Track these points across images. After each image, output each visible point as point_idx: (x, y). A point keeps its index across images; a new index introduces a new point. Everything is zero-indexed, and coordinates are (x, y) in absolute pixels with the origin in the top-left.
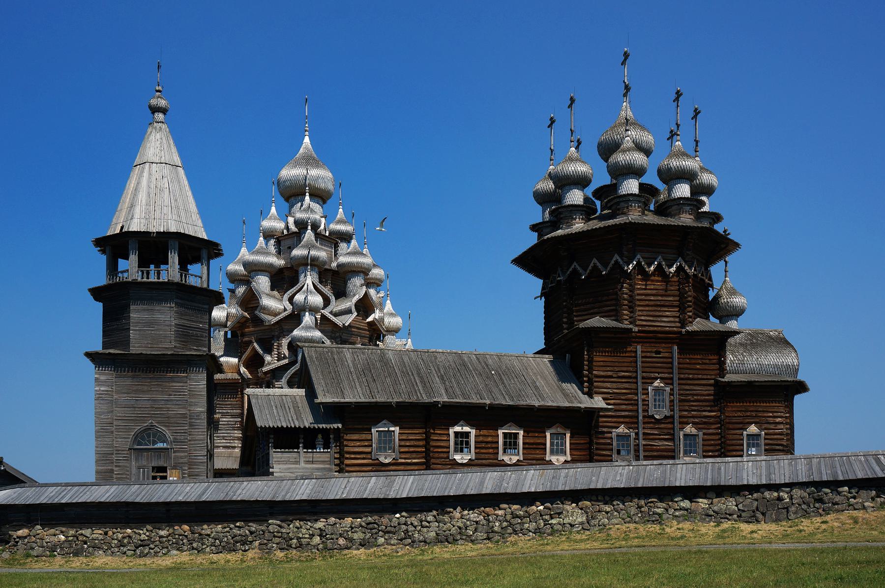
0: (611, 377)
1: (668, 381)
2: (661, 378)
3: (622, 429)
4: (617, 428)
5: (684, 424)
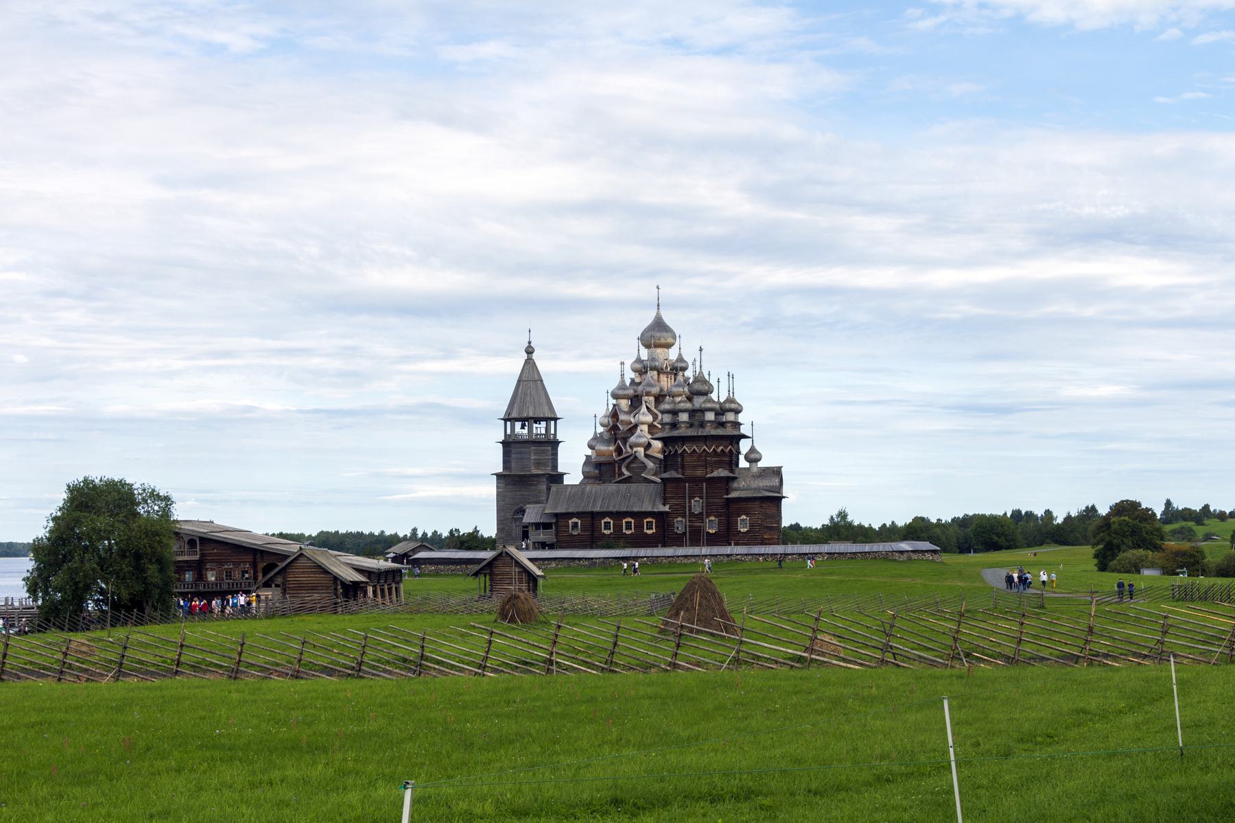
1: (701, 498)
5: (708, 516)
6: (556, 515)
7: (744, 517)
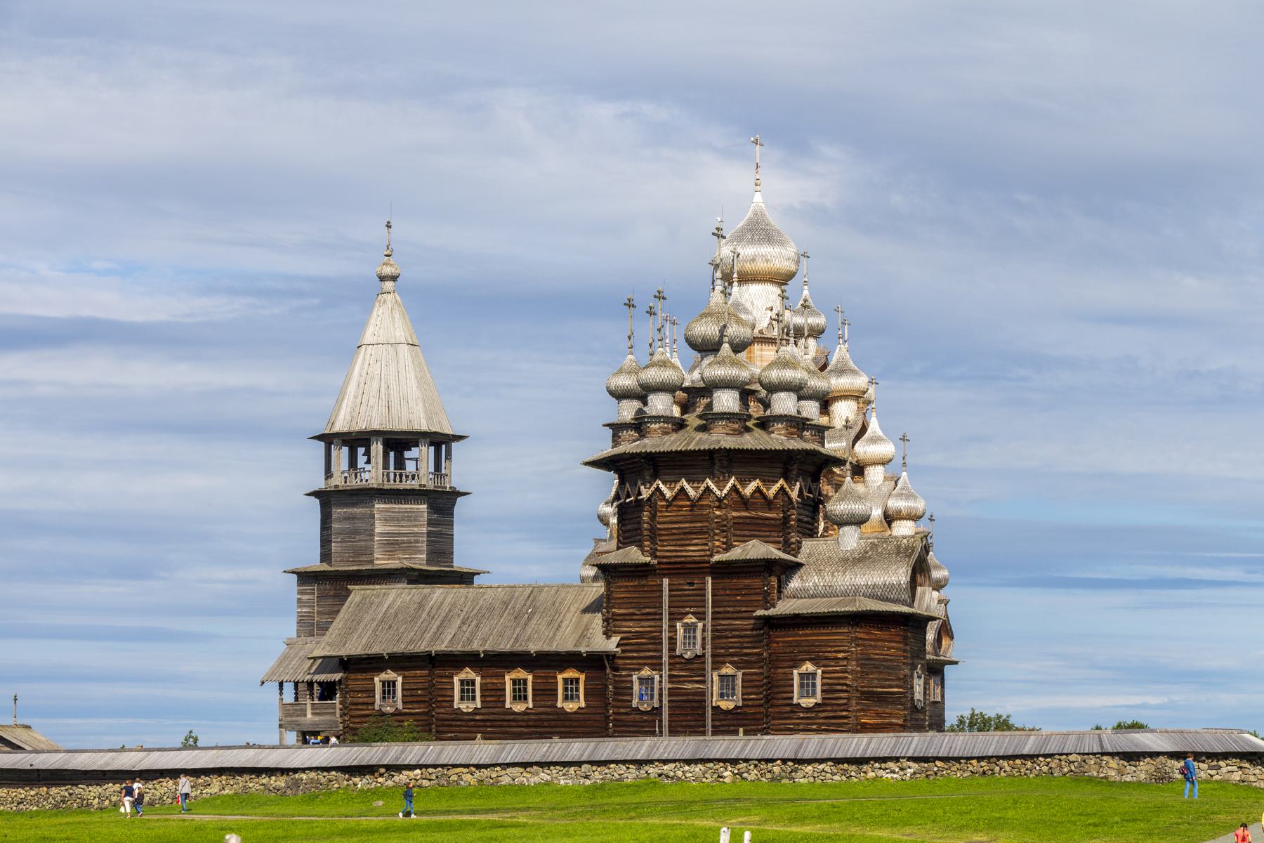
0: (634, 614)
1: (701, 616)
2: (693, 613)
3: (646, 672)
4: (639, 670)
5: (717, 665)
6: (348, 664)
7: (808, 667)
